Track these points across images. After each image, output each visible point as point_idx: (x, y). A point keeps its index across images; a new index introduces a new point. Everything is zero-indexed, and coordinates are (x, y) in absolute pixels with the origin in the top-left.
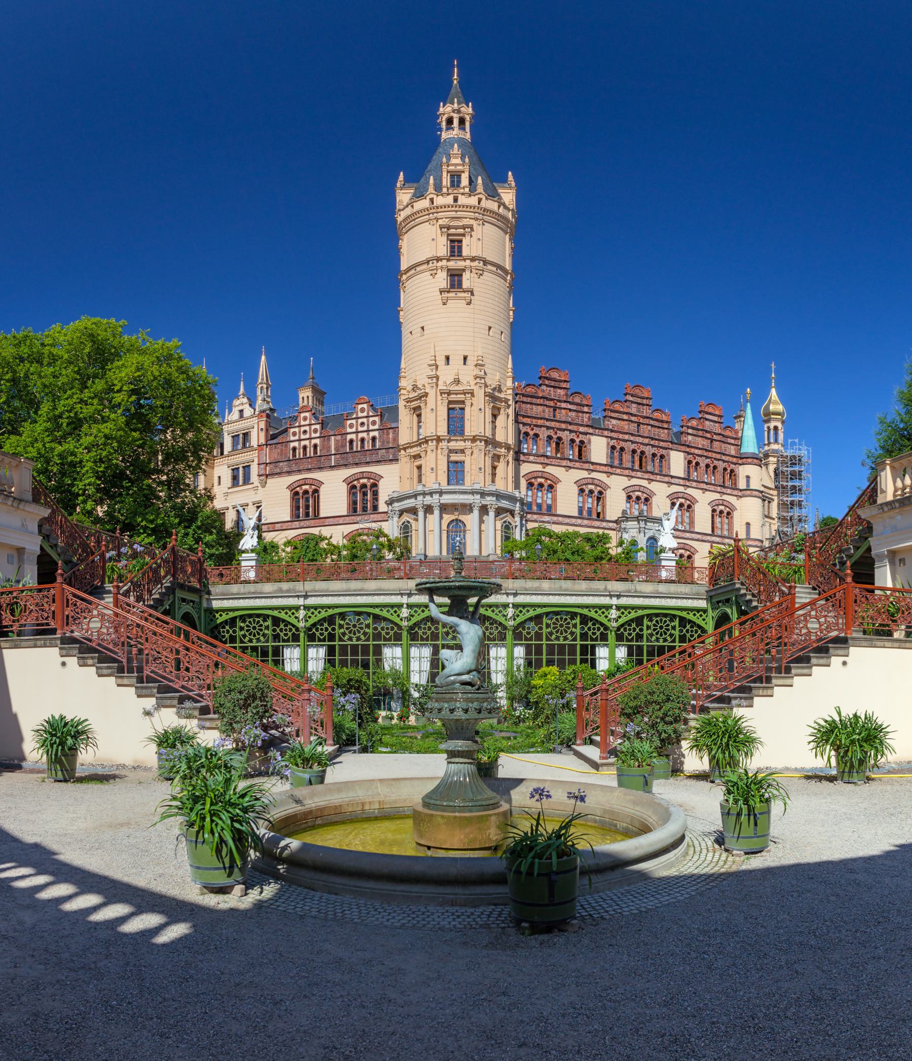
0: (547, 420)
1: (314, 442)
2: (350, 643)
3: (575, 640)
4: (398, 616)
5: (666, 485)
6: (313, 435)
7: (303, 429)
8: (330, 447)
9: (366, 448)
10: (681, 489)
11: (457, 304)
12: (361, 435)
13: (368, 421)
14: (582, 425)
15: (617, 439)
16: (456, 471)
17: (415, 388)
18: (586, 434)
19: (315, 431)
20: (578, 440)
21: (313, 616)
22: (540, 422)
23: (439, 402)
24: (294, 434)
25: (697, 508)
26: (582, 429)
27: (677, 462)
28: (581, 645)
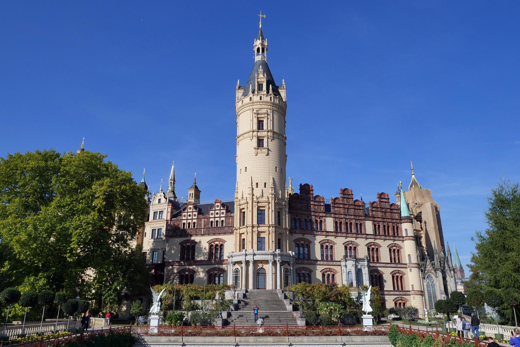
1: (194, 221)
6: (194, 217)
7: (189, 214)
9: (219, 226)
10: (372, 240)
12: (216, 219)
13: (220, 212)
14: (320, 212)
18: (322, 217)
19: (195, 215)
20: (319, 220)
23: (254, 207)
24: (185, 216)
26: (321, 215)
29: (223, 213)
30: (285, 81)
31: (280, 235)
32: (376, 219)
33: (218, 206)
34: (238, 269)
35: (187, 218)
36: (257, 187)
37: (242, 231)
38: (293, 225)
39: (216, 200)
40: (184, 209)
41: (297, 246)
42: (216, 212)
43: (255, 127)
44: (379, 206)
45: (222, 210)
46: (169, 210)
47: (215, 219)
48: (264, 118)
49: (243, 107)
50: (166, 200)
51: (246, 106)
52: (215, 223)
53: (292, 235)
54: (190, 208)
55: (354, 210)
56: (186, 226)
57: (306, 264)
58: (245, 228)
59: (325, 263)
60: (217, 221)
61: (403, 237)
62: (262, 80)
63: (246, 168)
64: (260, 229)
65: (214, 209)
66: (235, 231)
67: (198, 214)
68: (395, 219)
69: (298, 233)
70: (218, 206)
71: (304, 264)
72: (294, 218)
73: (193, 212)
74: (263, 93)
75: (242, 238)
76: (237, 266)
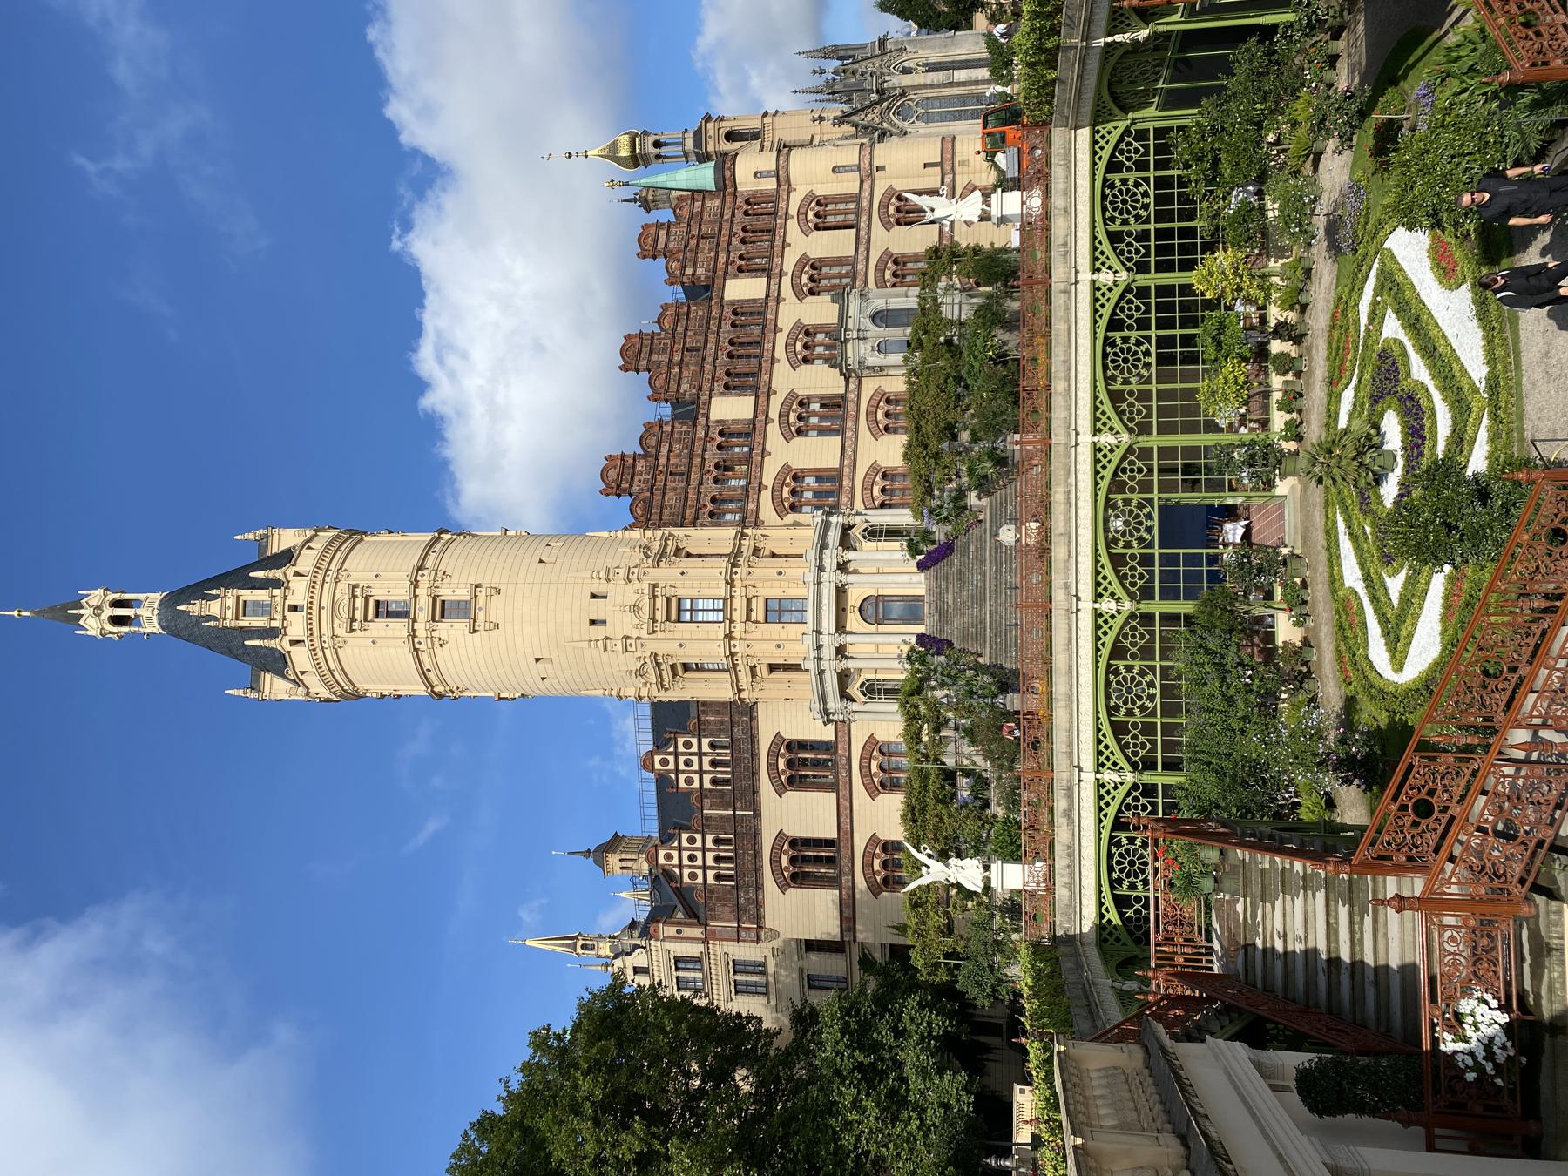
0: (688, 483)
1: (709, 844)
2: (1158, 700)
3: (1148, 339)
4: (1113, 617)
5: (781, 305)
6: (699, 844)
7: (686, 862)
8: (721, 817)
10: (786, 281)
11: (499, 609)
13: (683, 754)
14: (694, 433)
15: (713, 379)
16: (777, 611)
17: (641, 673)
19: (692, 840)
20: (719, 439)
21: (1113, 759)
22: (692, 495)
23: (670, 635)
24: (693, 876)
25: (816, 253)
26: (701, 433)
27: (742, 289)
28: (1157, 328)
29: (688, 745)
30: (242, 533)
32: (721, 266)
33: (664, 762)
34: (862, 685)
35: (699, 868)
36: (604, 622)
37: (744, 676)
39: (644, 767)
40: (668, 874)
42: (682, 767)
43: (399, 627)
44: (681, 255)
45: (676, 747)
46: (671, 931)
47: (706, 772)
48: (367, 599)
49: (325, 668)
50: (639, 946)
51: (321, 659)
54: (669, 857)
55: (689, 333)
56: (728, 869)
57: (853, 480)
59: (850, 424)
60: (713, 763)
61: (779, 185)
62: (230, 602)
63: (537, 660)
64: (739, 615)
65: (673, 776)
67: (688, 829)
68: (723, 209)
69: (758, 502)
70: (664, 762)
71: (853, 488)
72: (711, 514)
73: (680, 849)
74: (278, 599)
76: (854, 690)
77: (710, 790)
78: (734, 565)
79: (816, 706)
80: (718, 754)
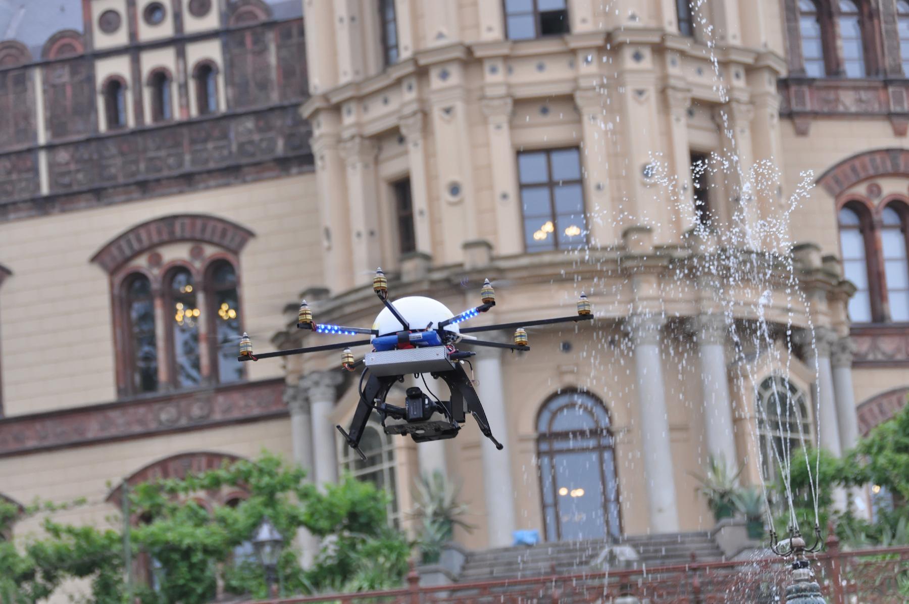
8: (28, 116)
9: (177, 115)
12: (150, 61)
31: (702, 118)
38: (811, 48)
41: (849, 218)
52: (147, 95)
53: (802, 133)
58: (398, 82)
60: (160, 78)
66: (323, 129)
75: (392, 168)
77: (91, 79)
78: (659, 50)
79: (310, 307)
80: (184, 87)
